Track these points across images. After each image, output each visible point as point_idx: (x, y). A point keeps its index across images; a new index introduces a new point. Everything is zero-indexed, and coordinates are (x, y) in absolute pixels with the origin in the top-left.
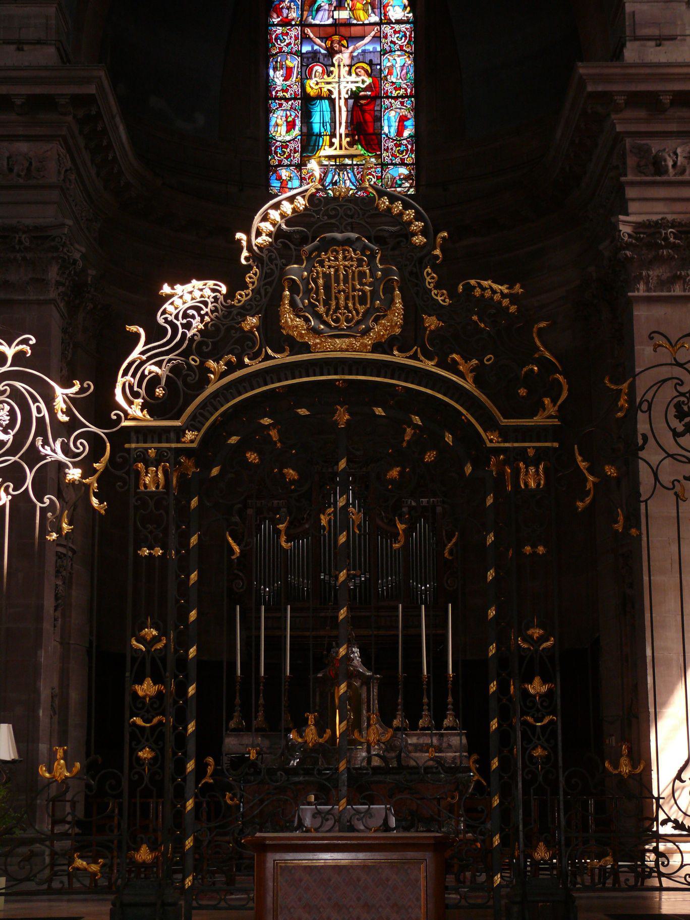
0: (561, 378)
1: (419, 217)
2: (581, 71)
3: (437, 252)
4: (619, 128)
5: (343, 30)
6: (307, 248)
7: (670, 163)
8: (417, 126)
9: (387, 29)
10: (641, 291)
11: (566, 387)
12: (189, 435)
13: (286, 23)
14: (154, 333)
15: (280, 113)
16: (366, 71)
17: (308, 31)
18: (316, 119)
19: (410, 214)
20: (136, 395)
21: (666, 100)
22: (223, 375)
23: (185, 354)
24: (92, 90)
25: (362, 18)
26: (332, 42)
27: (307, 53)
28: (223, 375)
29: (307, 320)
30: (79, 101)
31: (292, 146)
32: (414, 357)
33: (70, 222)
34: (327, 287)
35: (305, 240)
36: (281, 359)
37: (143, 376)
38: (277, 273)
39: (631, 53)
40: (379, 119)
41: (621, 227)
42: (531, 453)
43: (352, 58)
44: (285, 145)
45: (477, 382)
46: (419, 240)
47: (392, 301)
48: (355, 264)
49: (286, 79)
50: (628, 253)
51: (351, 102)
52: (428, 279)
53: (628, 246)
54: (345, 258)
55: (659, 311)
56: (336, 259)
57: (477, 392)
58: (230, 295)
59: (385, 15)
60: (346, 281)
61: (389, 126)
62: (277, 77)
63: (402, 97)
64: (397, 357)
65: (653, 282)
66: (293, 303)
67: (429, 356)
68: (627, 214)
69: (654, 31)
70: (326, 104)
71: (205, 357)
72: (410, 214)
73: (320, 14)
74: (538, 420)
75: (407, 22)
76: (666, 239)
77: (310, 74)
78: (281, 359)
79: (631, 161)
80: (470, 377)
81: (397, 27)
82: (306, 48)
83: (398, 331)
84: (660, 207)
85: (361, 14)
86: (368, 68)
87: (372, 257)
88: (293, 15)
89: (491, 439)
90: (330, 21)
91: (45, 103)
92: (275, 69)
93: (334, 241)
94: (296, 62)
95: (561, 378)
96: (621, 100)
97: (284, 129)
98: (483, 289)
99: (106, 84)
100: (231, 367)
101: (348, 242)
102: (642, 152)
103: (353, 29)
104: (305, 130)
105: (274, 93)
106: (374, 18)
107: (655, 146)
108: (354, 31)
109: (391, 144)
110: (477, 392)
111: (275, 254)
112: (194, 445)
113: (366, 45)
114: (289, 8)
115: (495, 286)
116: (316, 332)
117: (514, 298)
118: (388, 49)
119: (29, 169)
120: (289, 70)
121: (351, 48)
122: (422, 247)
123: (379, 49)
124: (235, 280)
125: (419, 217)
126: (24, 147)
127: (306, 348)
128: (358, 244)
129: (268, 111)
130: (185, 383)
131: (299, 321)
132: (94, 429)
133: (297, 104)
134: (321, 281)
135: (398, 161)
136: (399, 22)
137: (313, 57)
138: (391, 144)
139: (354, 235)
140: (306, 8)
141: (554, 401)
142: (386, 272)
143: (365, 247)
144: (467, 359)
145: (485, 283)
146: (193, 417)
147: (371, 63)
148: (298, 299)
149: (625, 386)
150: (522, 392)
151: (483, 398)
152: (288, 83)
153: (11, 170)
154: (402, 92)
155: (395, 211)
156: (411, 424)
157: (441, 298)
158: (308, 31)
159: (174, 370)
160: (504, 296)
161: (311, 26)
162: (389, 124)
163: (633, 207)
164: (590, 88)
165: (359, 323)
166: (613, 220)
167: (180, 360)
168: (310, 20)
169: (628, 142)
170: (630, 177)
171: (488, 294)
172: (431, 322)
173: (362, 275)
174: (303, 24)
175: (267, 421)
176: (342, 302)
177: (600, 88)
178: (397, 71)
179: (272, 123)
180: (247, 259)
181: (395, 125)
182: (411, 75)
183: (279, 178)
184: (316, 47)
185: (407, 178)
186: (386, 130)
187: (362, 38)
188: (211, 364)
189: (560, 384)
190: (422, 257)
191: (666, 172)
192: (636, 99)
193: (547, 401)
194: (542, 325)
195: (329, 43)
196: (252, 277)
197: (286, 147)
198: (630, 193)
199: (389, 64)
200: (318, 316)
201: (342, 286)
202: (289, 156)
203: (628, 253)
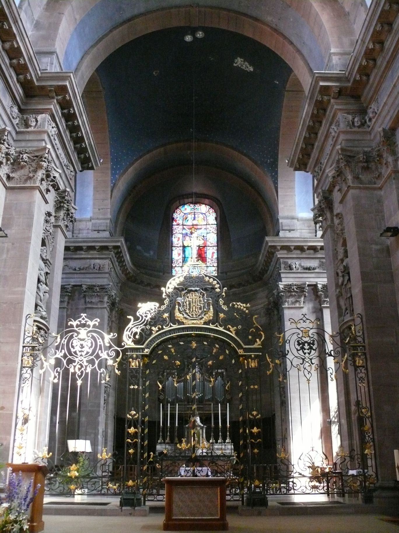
0: (262, 333)
1: (218, 283)
2: (267, 239)
3: (224, 294)
4: (279, 256)
5: (195, 226)
6: (183, 292)
7: (294, 267)
10: (286, 305)
11: (263, 336)
12: (146, 350)
14: (136, 318)
19: (215, 282)
20: (130, 338)
21: (292, 248)
22: (157, 331)
23: (146, 325)
24: (119, 244)
28: (157, 331)
29: (183, 315)
31: (179, 261)
32: (217, 326)
33: (111, 284)
34: (190, 304)
35: (183, 290)
37: (132, 332)
38: (174, 300)
39: (281, 234)
40: (206, 253)
41: (280, 286)
42: (253, 356)
45: (236, 334)
47: (210, 309)
48: (198, 297)
49: (178, 241)
50: (282, 294)
52: (221, 302)
53: (282, 292)
54: (195, 296)
55: (292, 311)
56: (192, 296)
57: (236, 337)
58: (160, 307)
60: (195, 303)
62: (175, 240)
64: (211, 326)
65: (290, 302)
66: (179, 309)
67: (221, 326)
68: (282, 282)
69: (288, 228)
71: (151, 326)
72: (215, 282)
74: (256, 346)
76: (293, 289)
79: (283, 266)
80: (234, 332)
82: (184, 232)
83: (211, 318)
84: (292, 280)
86: (203, 238)
87: (203, 295)
88: (180, 222)
89: (241, 352)
91: (105, 248)
93: (191, 291)
95: (262, 333)
96: (279, 248)
97: (177, 255)
98: (238, 305)
99: (123, 242)
100: (160, 329)
101: (196, 291)
102: (286, 263)
104: (183, 256)
107: (290, 261)
108: (199, 227)
109: (210, 260)
110: (236, 337)
111: (174, 294)
112: (148, 353)
115: (241, 304)
116: (186, 318)
117: (247, 308)
119: (99, 268)
120: (179, 238)
122: (218, 293)
124: (161, 303)
125: (218, 283)
126: (98, 261)
128: (199, 291)
129: (172, 250)
130: (145, 334)
131: (181, 315)
132: (116, 348)
134: (188, 303)
135: (212, 265)
137: (186, 234)
139: (198, 289)
141: (260, 340)
142: (208, 300)
143: (201, 292)
144: (233, 327)
145: (238, 304)
146: (148, 345)
147: (203, 236)
148: (180, 308)
149: (282, 335)
150: (250, 337)
151: (238, 339)
153: (94, 268)
154: (213, 245)
155: (211, 281)
156: (215, 347)
157: (225, 308)
158: (184, 227)
159: (142, 330)
160: (244, 307)
163: (283, 280)
164: (269, 244)
165: (199, 316)
166: (277, 284)
167: (144, 327)
169: (281, 260)
170: (282, 271)
171: (239, 307)
173: (200, 301)
174: (183, 225)
175: (170, 346)
176: (194, 309)
177: (273, 244)
180: (165, 296)
182: (216, 240)
184: (187, 232)
186: (208, 256)
188: (153, 328)
189: (262, 335)
190: (219, 296)
191: (293, 269)
192: (283, 248)
193: (258, 340)
194: (256, 316)
195: (191, 230)
196: (167, 302)
198: (282, 275)
200: (187, 313)
201: (194, 304)
203: (282, 294)
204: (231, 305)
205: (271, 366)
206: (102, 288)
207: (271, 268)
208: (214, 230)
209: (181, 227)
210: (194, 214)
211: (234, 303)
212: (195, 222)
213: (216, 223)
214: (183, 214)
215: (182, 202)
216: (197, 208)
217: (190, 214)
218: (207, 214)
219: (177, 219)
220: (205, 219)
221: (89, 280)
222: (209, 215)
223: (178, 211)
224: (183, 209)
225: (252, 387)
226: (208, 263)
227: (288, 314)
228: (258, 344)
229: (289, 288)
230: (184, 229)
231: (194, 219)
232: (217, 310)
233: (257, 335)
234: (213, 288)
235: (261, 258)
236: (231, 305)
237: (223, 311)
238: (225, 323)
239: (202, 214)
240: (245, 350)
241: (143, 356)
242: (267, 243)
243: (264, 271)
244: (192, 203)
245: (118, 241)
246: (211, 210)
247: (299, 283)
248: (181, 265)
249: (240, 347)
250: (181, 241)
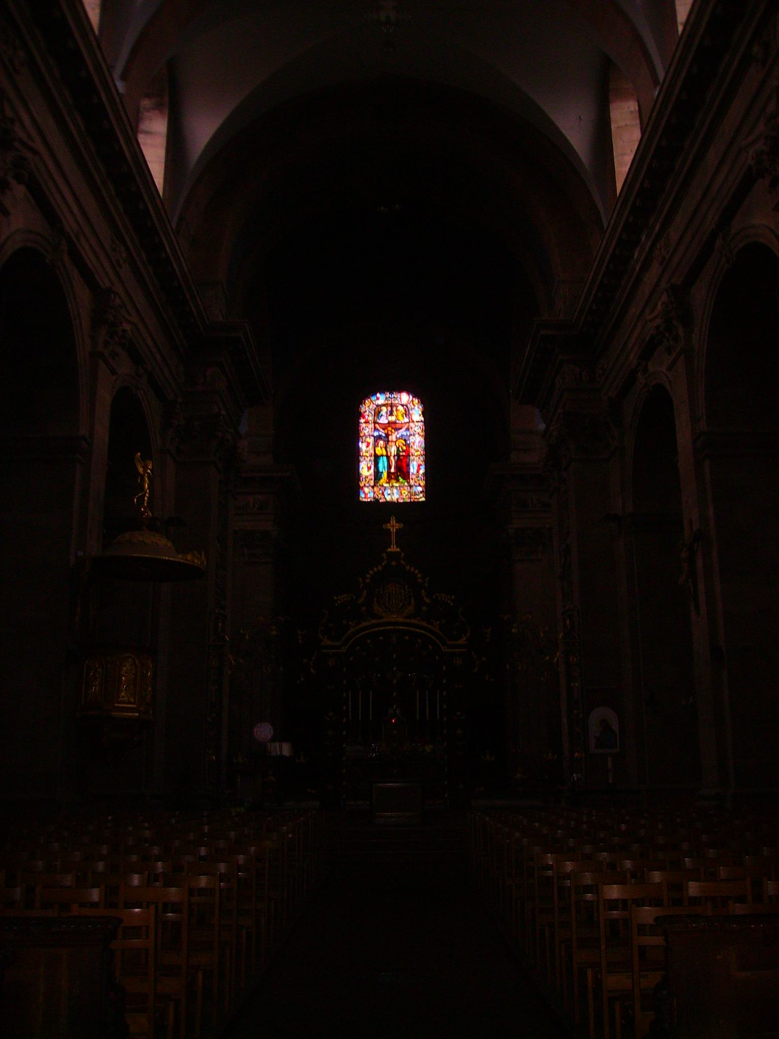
5: (393, 426)
8: (426, 469)
9: (412, 425)
13: (367, 422)
15: (364, 462)
16: (403, 444)
17: (377, 426)
18: (381, 466)
25: (401, 420)
26: (388, 431)
27: (377, 436)
31: (369, 478)
36: (374, 621)
40: (408, 465)
43: (397, 438)
44: (367, 477)
46: (420, 580)
51: (396, 458)
56: (392, 587)
59: (411, 419)
61: (414, 468)
62: (363, 446)
63: (419, 455)
70: (385, 458)
73: (382, 417)
74: (460, 642)
75: (422, 421)
77: (378, 444)
81: (417, 424)
82: (376, 434)
85: (400, 418)
86: (404, 442)
88: (371, 418)
90: (386, 422)
92: (362, 442)
94: (371, 440)
97: (366, 469)
103: (397, 425)
104: (376, 470)
105: (361, 454)
106: (406, 420)
108: (398, 426)
109: (414, 477)
113: (402, 432)
114: (368, 416)
118: (412, 433)
120: (368, 444)
121: (396, 433)
123: (408, 434)
127: (382, 618)
129: (359, 462)
133: (373, 458)
134: (387, 595)
136: (417, 422)
137: (380, 437)
138: (414, 477)
140: (376, 415)
141: (465, 636)
145: (443, 595)
149: (489, 630)
152: (368, 449)
154: (419, 453)
158: (377, 426)
161: (378, 423)
162: (413, 469)
168: (378, 420)
178: (417, 444)
179: (361, 467)
181: (416, 468)
182: (423, 445)
183: (364, 492)
184: (380, 433)
185: (421, 492)
187: (401, 429)
195: (386, 431)
197: (367, 478)
199: (413, 441)
202: (369, 482)
204: (434, 597)
208: (420, 431)
209: (371, 426)
210: (392, 407)
211: (438, 595)
213: (423, 419)
214: (375, 406)
216: (396, 397)
217: (384, 405)
218: (410, 406)
219: (365, 414)
220: (407, 413)
222: (413, 407)
224: (374, 398)
225: (456, 686)
226: (411, 481)
230: (376, 429)
231: (391, 414)
236: (434, 597)
239: (403, 405)
246: (416, 401)
248: (372, 483)
250: (371, 446)
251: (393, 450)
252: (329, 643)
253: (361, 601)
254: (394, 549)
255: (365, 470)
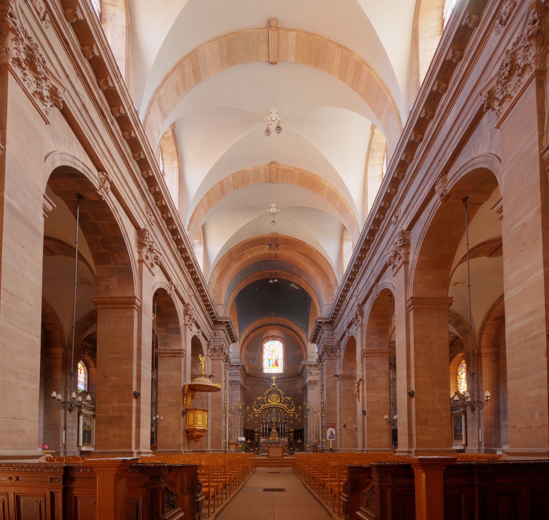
24: (244, 364)
30: (242, 365)
39: (309, 360)
47: (278, 399)
55: (311, 390)
64: (279, 404)
78: (269, 404)
79: (308, 372)
82: (269, 353)
84: (311, 378)
89: (288, 412)
91: (239, 365)
102: (309, 371)
126: (236, 371)
127: (270, 403)
157: (283, 399)
163: (308, 378)
172: (282, 401)
190: (282, 395)
196: (266, 397)
198: (308, 376)
205: (297, 416)
206: (238, 381)
207: (304, 372)
212: (274, 349)
215: (268, 339)
221: (232, 378)
223: (266, 343)
227: (309, 391)
228: (293, 410)
229: (310, 382)
232: (281, 400)
233: (293, 407)
234: (280, 392)
235: (300, 368)
237: (283, 400)
238: (283, 403)
240: (289, 411)
241: (259, 413)
242: (302, 363)
243: (301, 373)
244: (273, 340)
245: (243, 363)
246: (281, 343)
247: (315, 380)
249: (288, 410)
251: (274, 358)
252: (256, 410)
253: (265, 399)
254: (274, 384)
255: (265, 364)
